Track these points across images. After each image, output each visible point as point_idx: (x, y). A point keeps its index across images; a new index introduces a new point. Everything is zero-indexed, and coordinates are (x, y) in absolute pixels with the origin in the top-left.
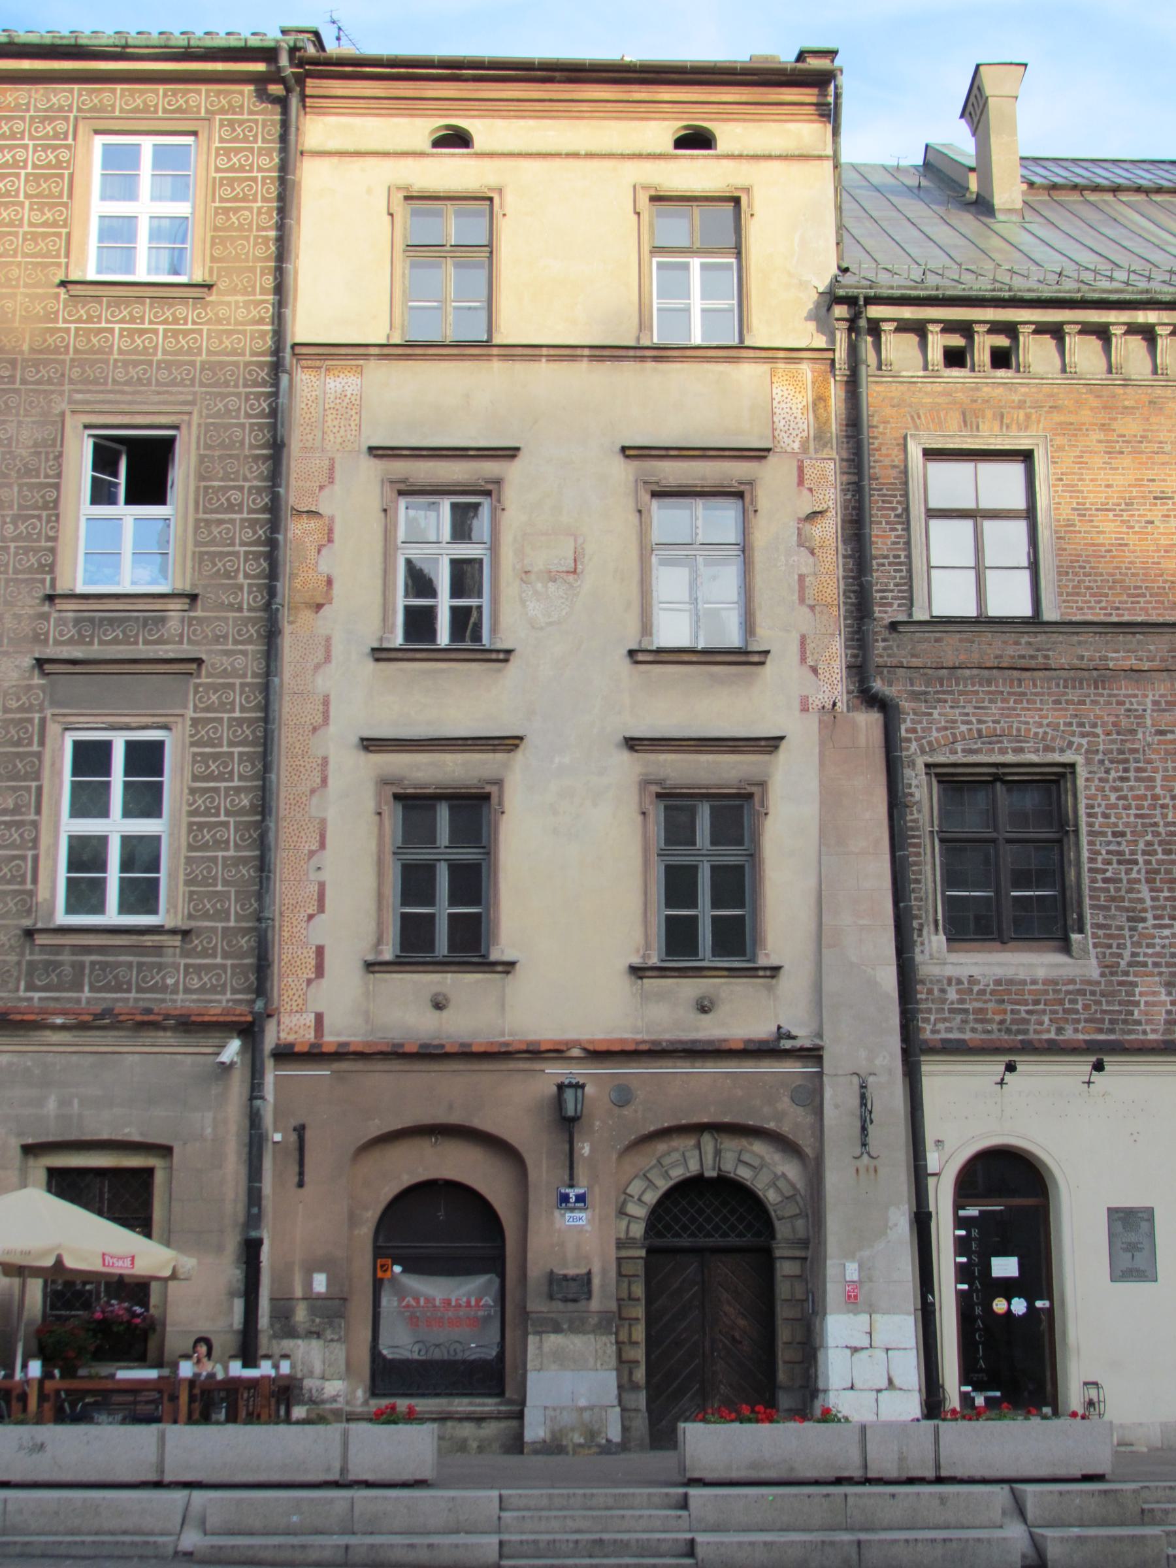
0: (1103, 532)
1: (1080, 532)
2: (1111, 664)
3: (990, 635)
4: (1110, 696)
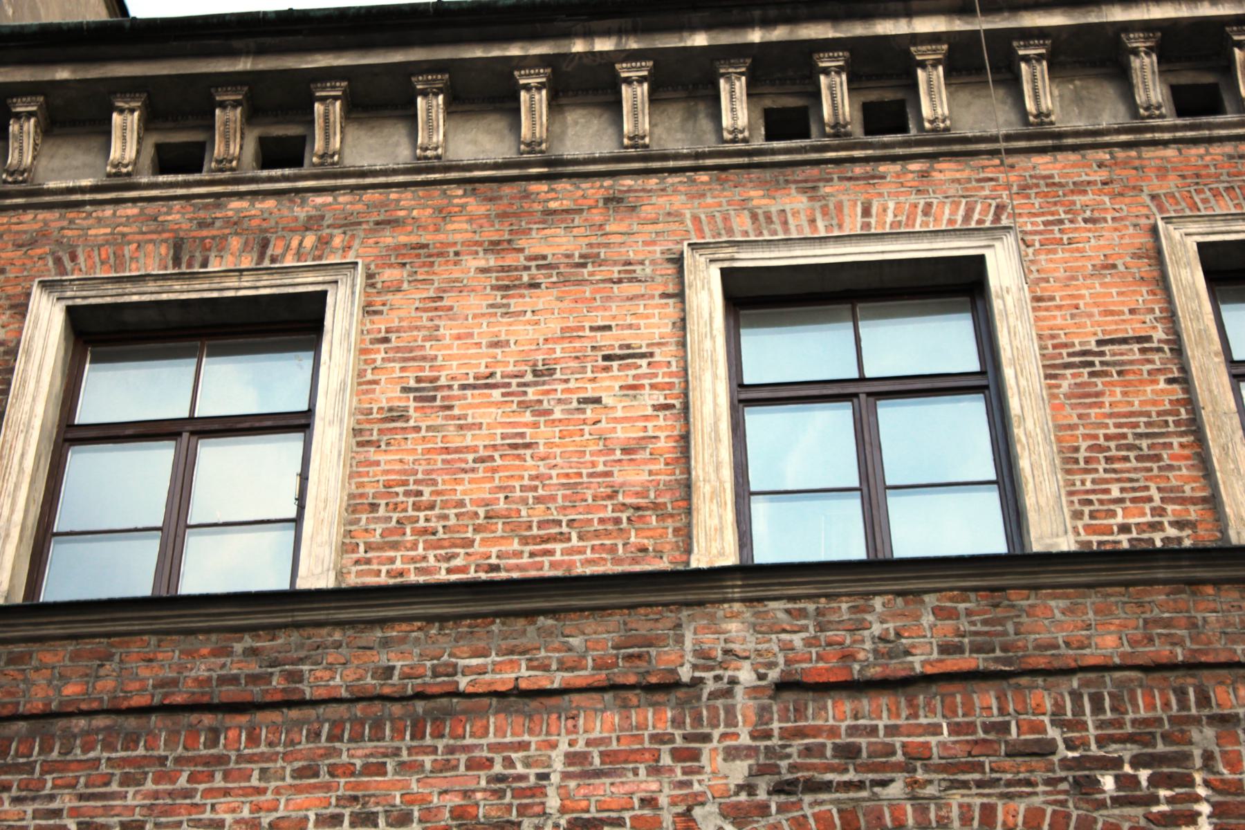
0: (480, 426)
1: (417, 429)
2: (463, 683)
3: (153, 640)
4: (451, 750)
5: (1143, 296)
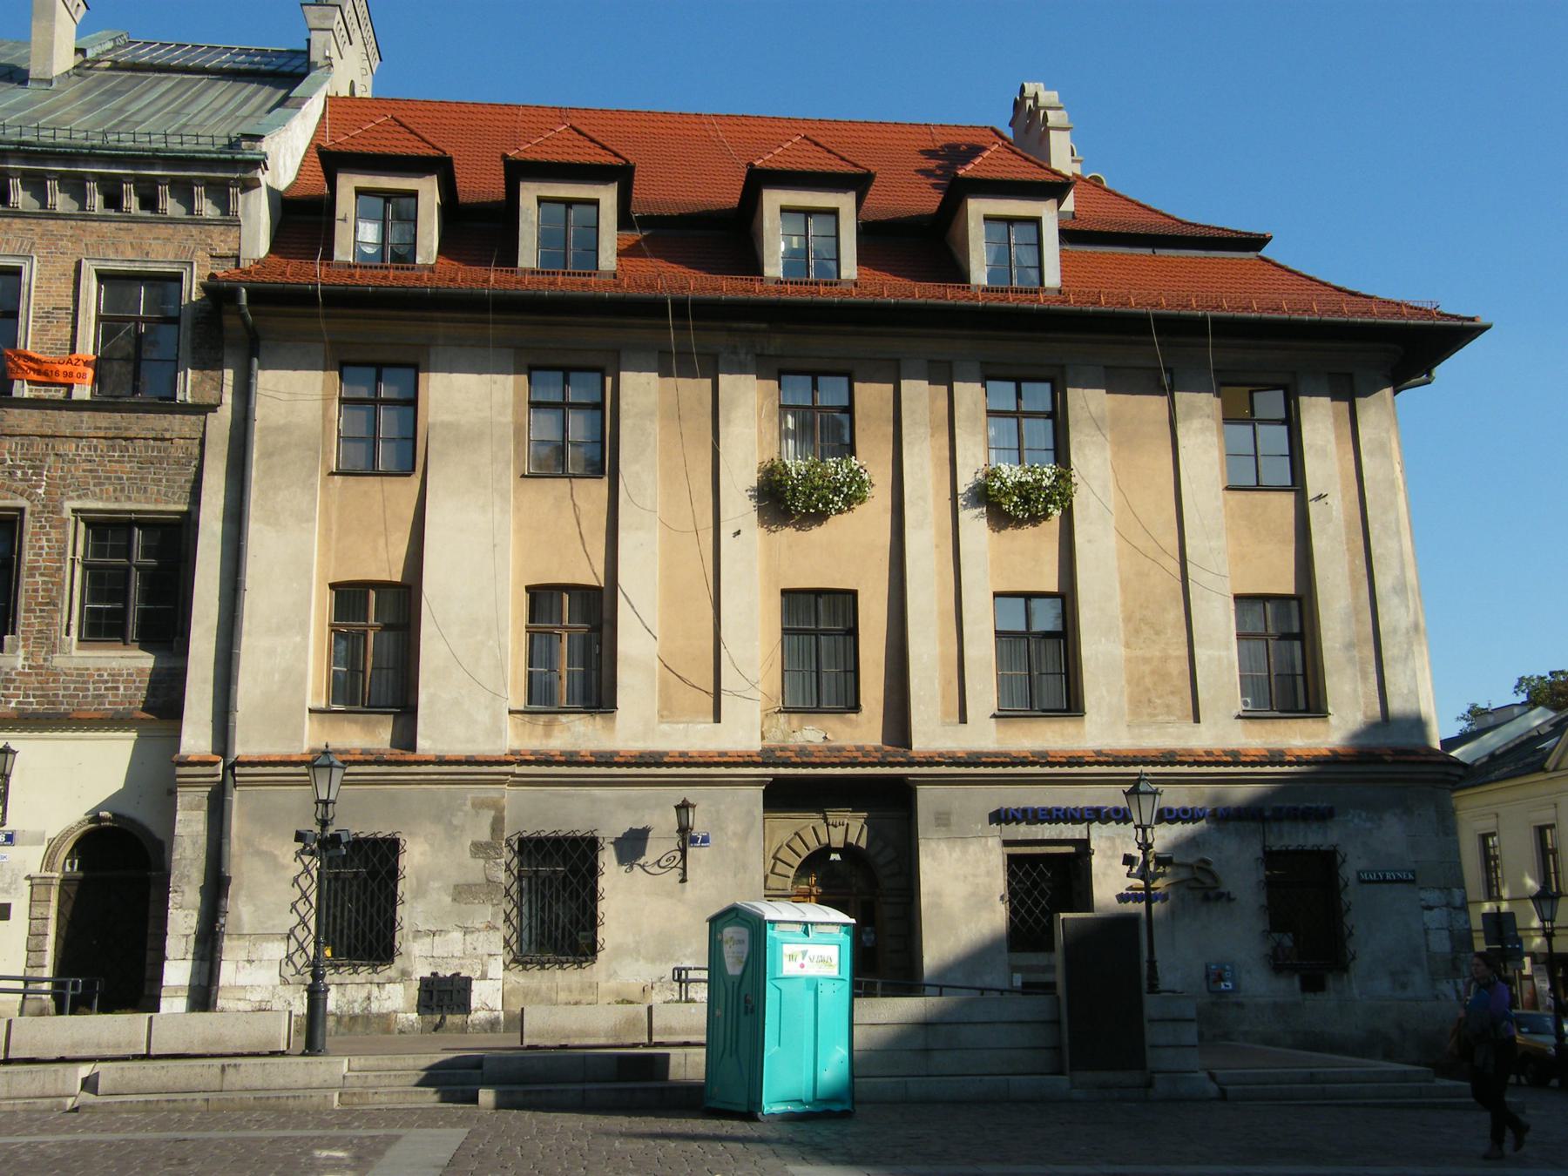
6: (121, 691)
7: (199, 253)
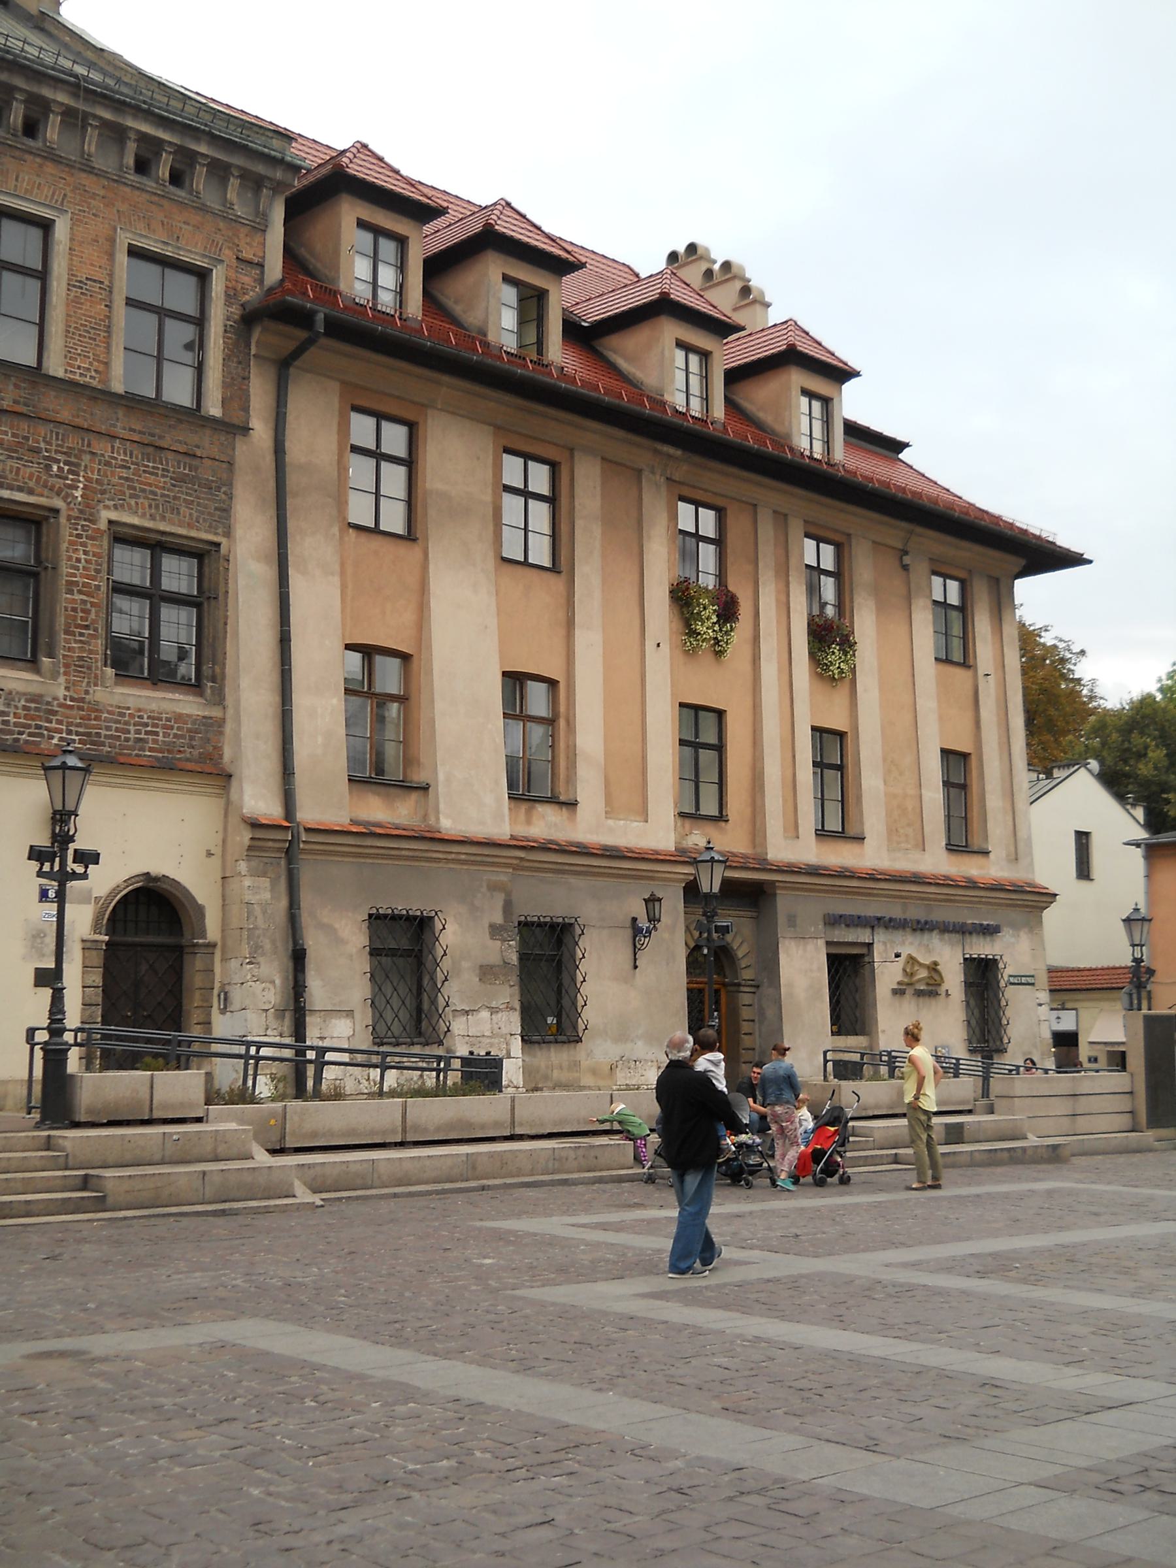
5: (104, 261)
6: (161, 738)
7: (227, 252)
